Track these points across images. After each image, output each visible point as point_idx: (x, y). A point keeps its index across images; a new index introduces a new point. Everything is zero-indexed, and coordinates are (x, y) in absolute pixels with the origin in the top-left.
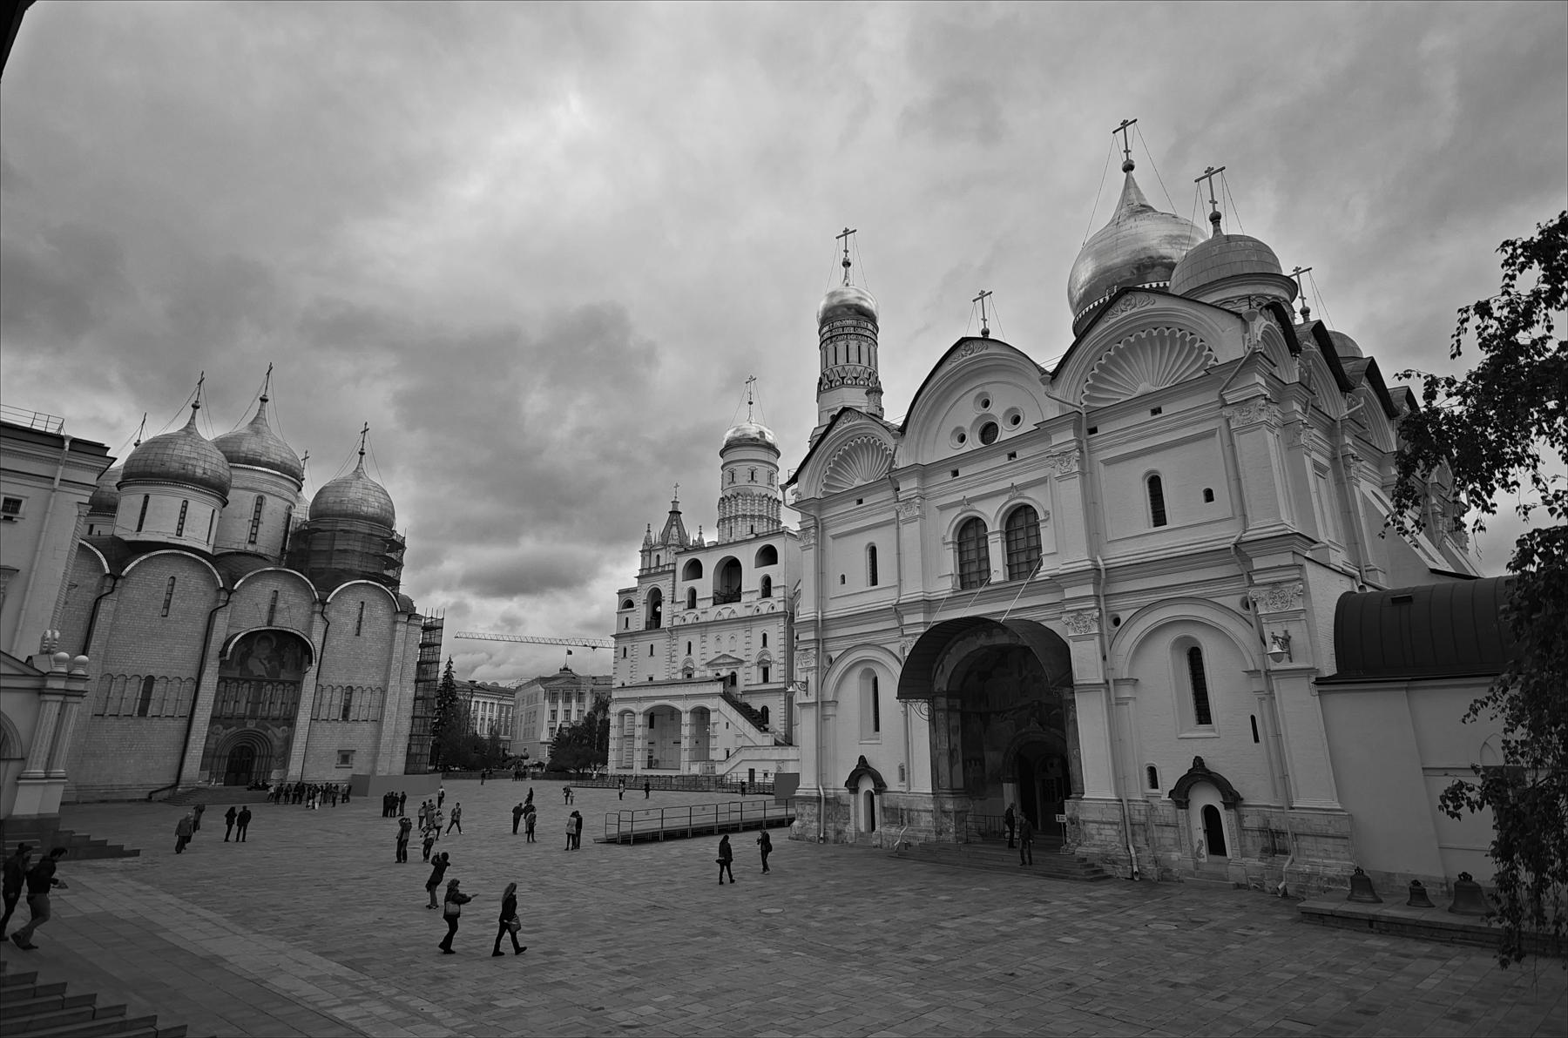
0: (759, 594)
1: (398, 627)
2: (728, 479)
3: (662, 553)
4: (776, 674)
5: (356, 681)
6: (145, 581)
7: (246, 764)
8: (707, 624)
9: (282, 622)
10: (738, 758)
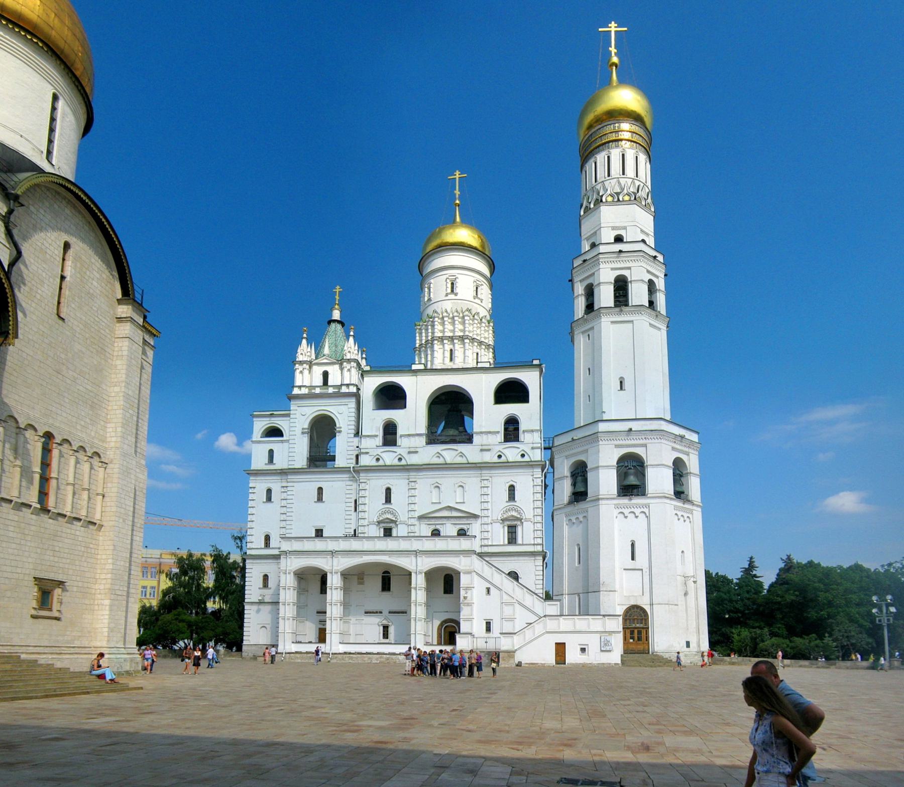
0: (501, 437)
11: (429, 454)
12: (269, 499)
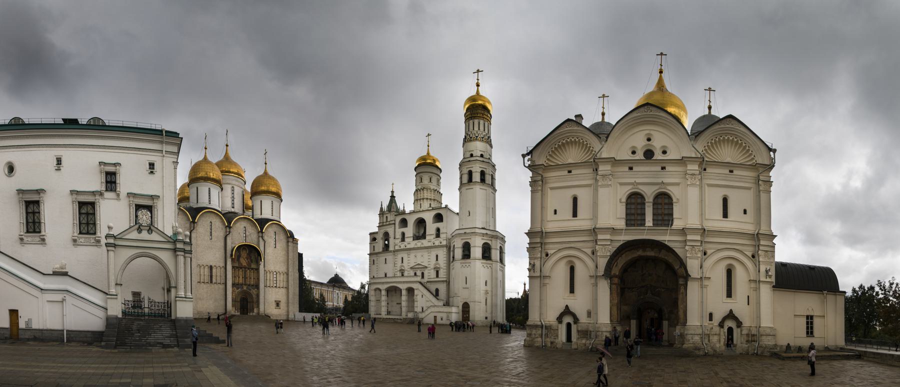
2: (419, 180)
3: (388, 215)
4: (442, 274)
6: (203, 223)
7: (247, 301)
8: (410, 249)
10: (429, 311)
11: (413, 244)
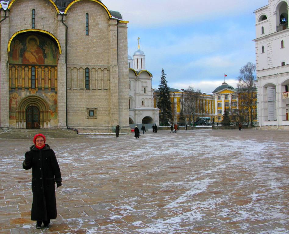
1: (111, 28)
5: (91, 64)
9: (40, 27)
12: (263, 51)
